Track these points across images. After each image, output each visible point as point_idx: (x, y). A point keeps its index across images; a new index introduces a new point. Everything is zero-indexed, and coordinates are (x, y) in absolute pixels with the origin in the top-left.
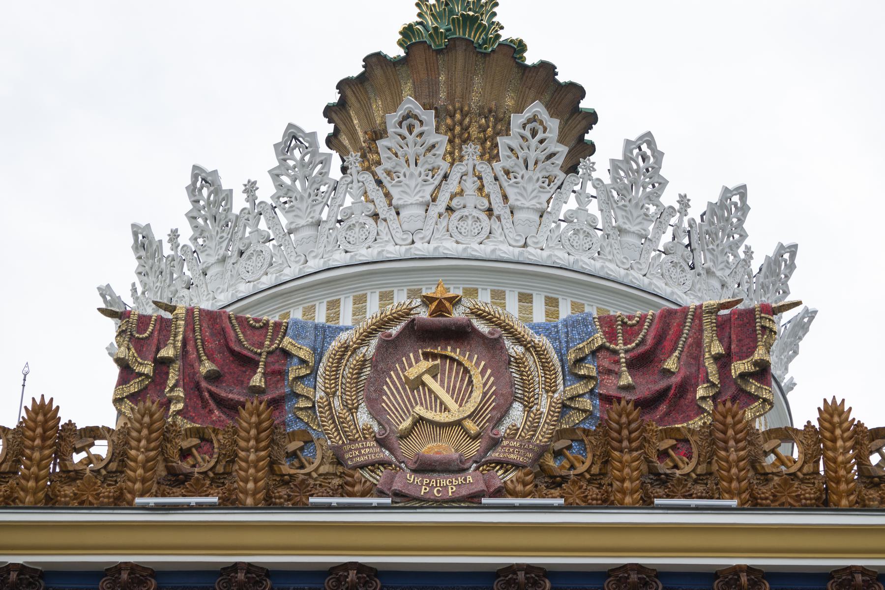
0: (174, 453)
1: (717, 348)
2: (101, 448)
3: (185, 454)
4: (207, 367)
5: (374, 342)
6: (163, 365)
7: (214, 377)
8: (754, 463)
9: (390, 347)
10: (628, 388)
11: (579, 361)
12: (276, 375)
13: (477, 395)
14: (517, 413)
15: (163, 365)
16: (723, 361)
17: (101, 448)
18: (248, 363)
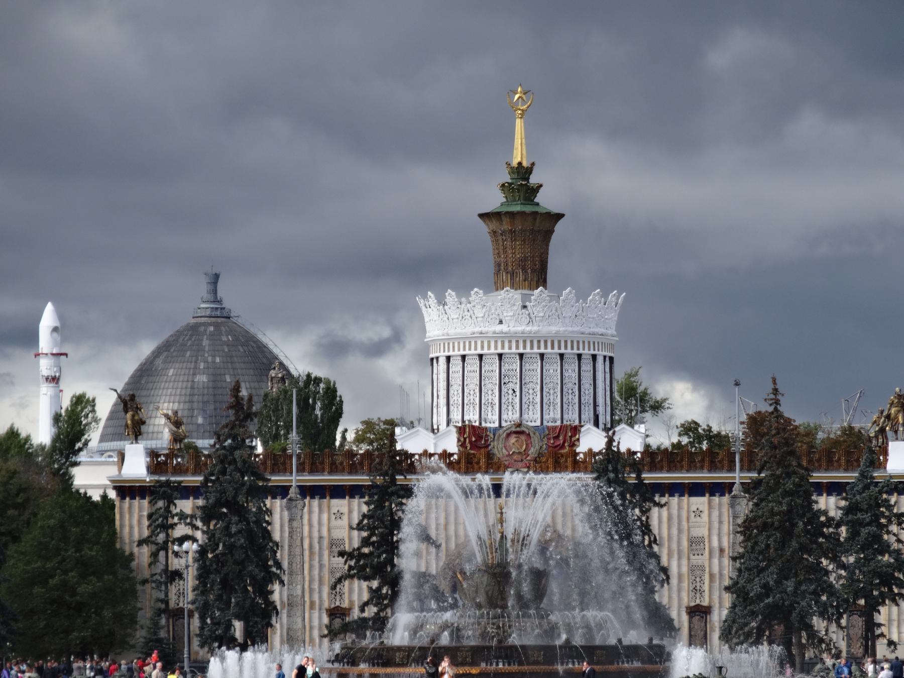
0: (469, 458)
1: (570, 434)
2: (456, 457)
3: (472, 458)
4: (474, 439)
5: (505, 434)
6: (465, 439)
7: (475, 441)
8: (575, 459)
9: (508, 435)
10: (553, 443)
11: (544, 438)
12: (486, 441)
13: (524, 447)
14: (532, 449)
15: (465, 439)
16: (571, 437)
17: (456, 457)
18: (481, 438)
